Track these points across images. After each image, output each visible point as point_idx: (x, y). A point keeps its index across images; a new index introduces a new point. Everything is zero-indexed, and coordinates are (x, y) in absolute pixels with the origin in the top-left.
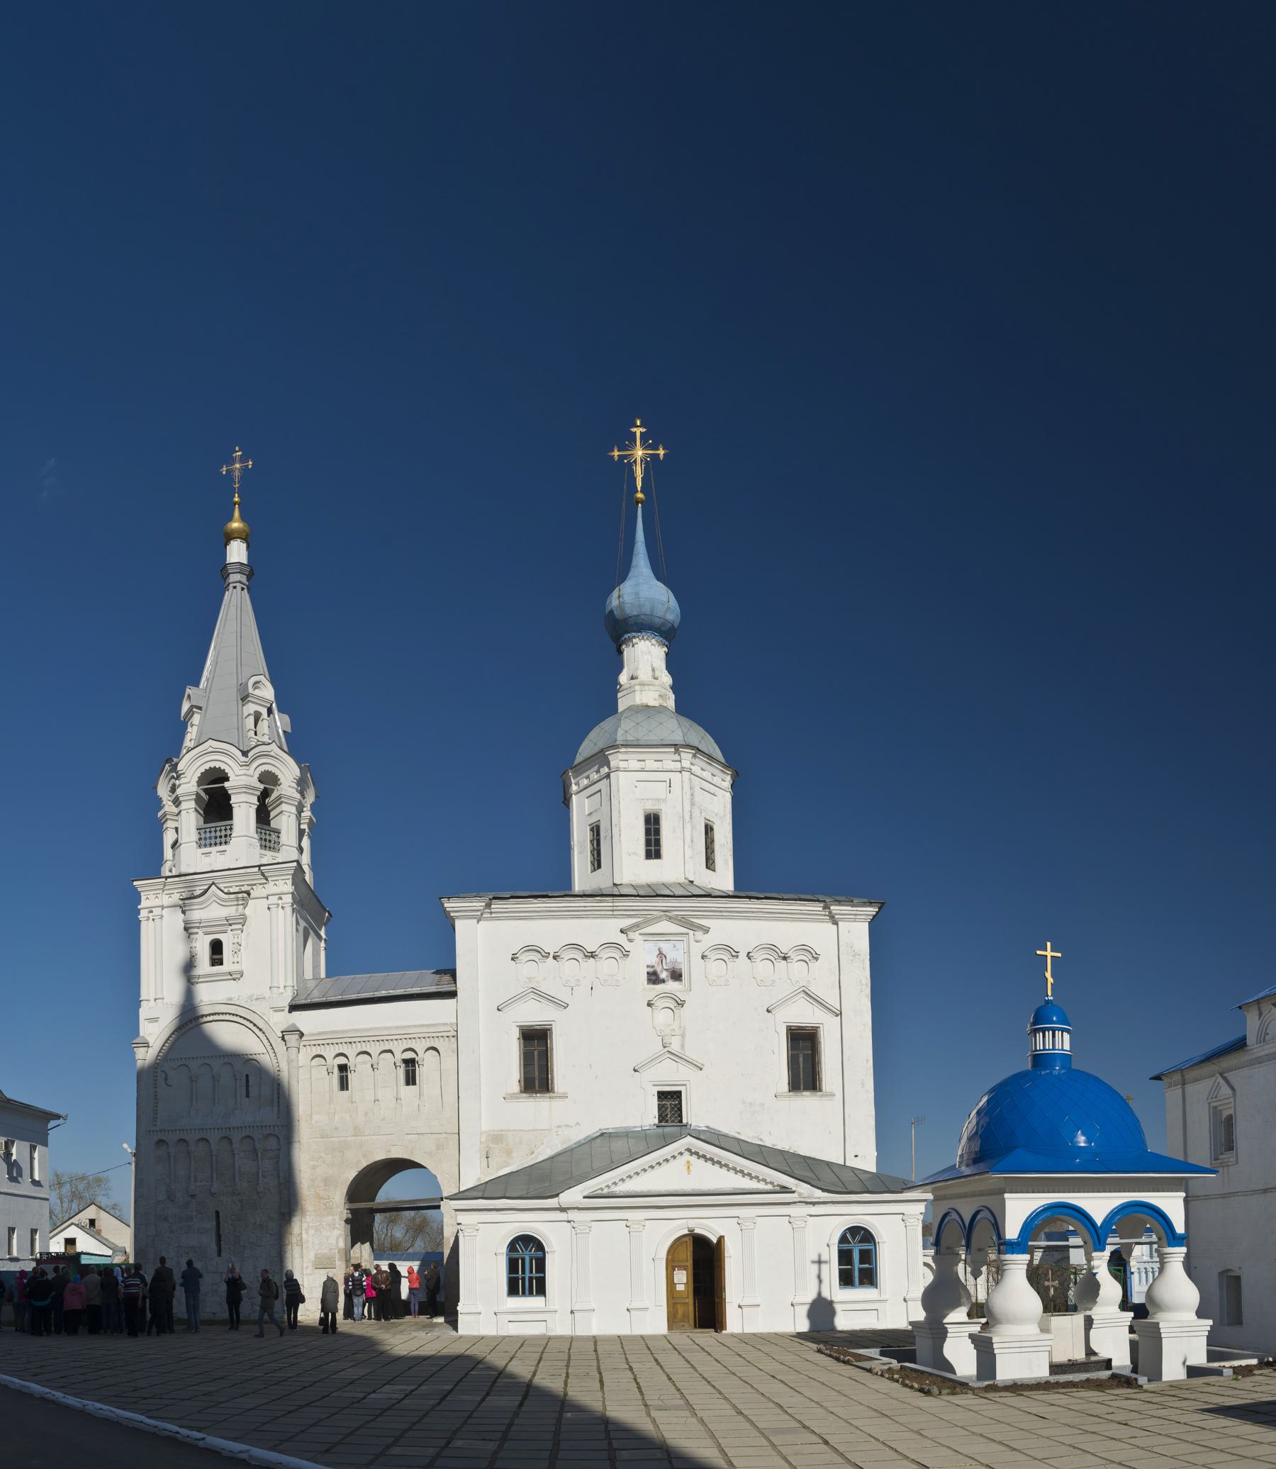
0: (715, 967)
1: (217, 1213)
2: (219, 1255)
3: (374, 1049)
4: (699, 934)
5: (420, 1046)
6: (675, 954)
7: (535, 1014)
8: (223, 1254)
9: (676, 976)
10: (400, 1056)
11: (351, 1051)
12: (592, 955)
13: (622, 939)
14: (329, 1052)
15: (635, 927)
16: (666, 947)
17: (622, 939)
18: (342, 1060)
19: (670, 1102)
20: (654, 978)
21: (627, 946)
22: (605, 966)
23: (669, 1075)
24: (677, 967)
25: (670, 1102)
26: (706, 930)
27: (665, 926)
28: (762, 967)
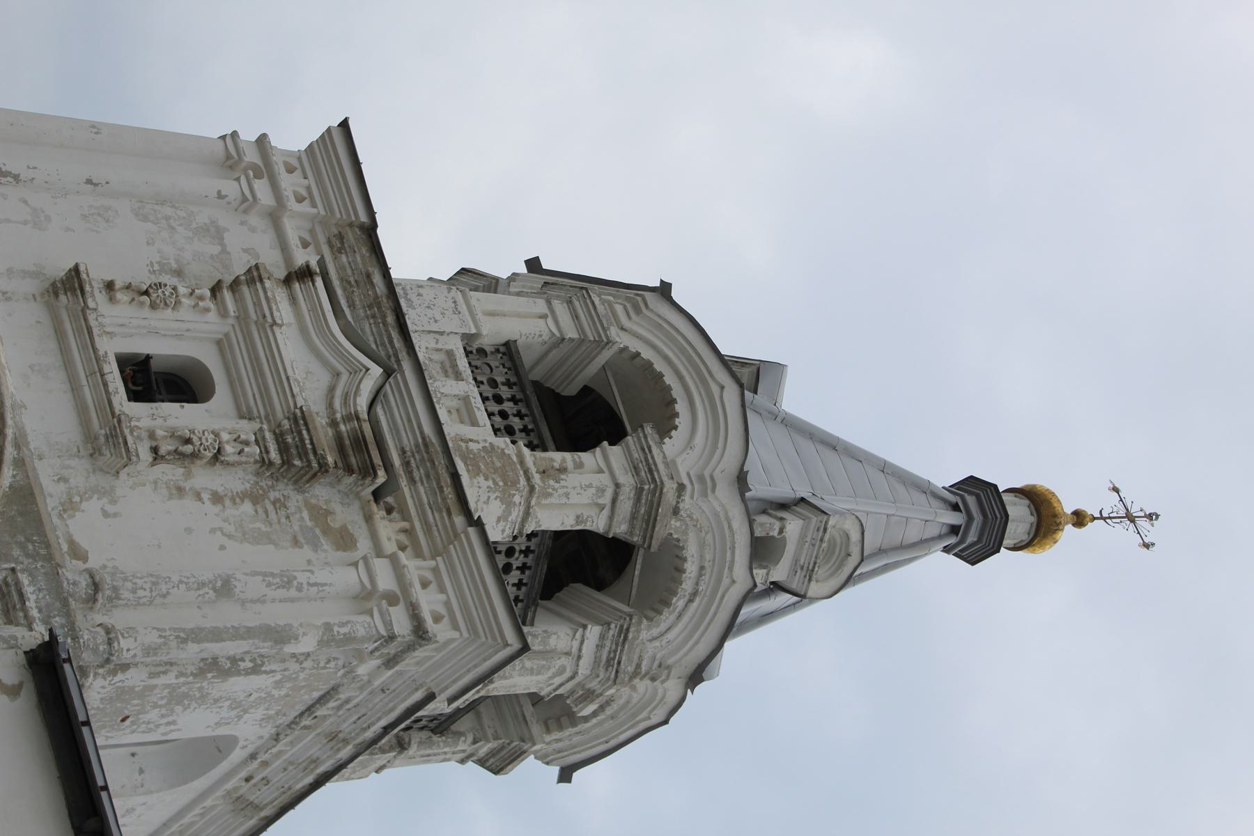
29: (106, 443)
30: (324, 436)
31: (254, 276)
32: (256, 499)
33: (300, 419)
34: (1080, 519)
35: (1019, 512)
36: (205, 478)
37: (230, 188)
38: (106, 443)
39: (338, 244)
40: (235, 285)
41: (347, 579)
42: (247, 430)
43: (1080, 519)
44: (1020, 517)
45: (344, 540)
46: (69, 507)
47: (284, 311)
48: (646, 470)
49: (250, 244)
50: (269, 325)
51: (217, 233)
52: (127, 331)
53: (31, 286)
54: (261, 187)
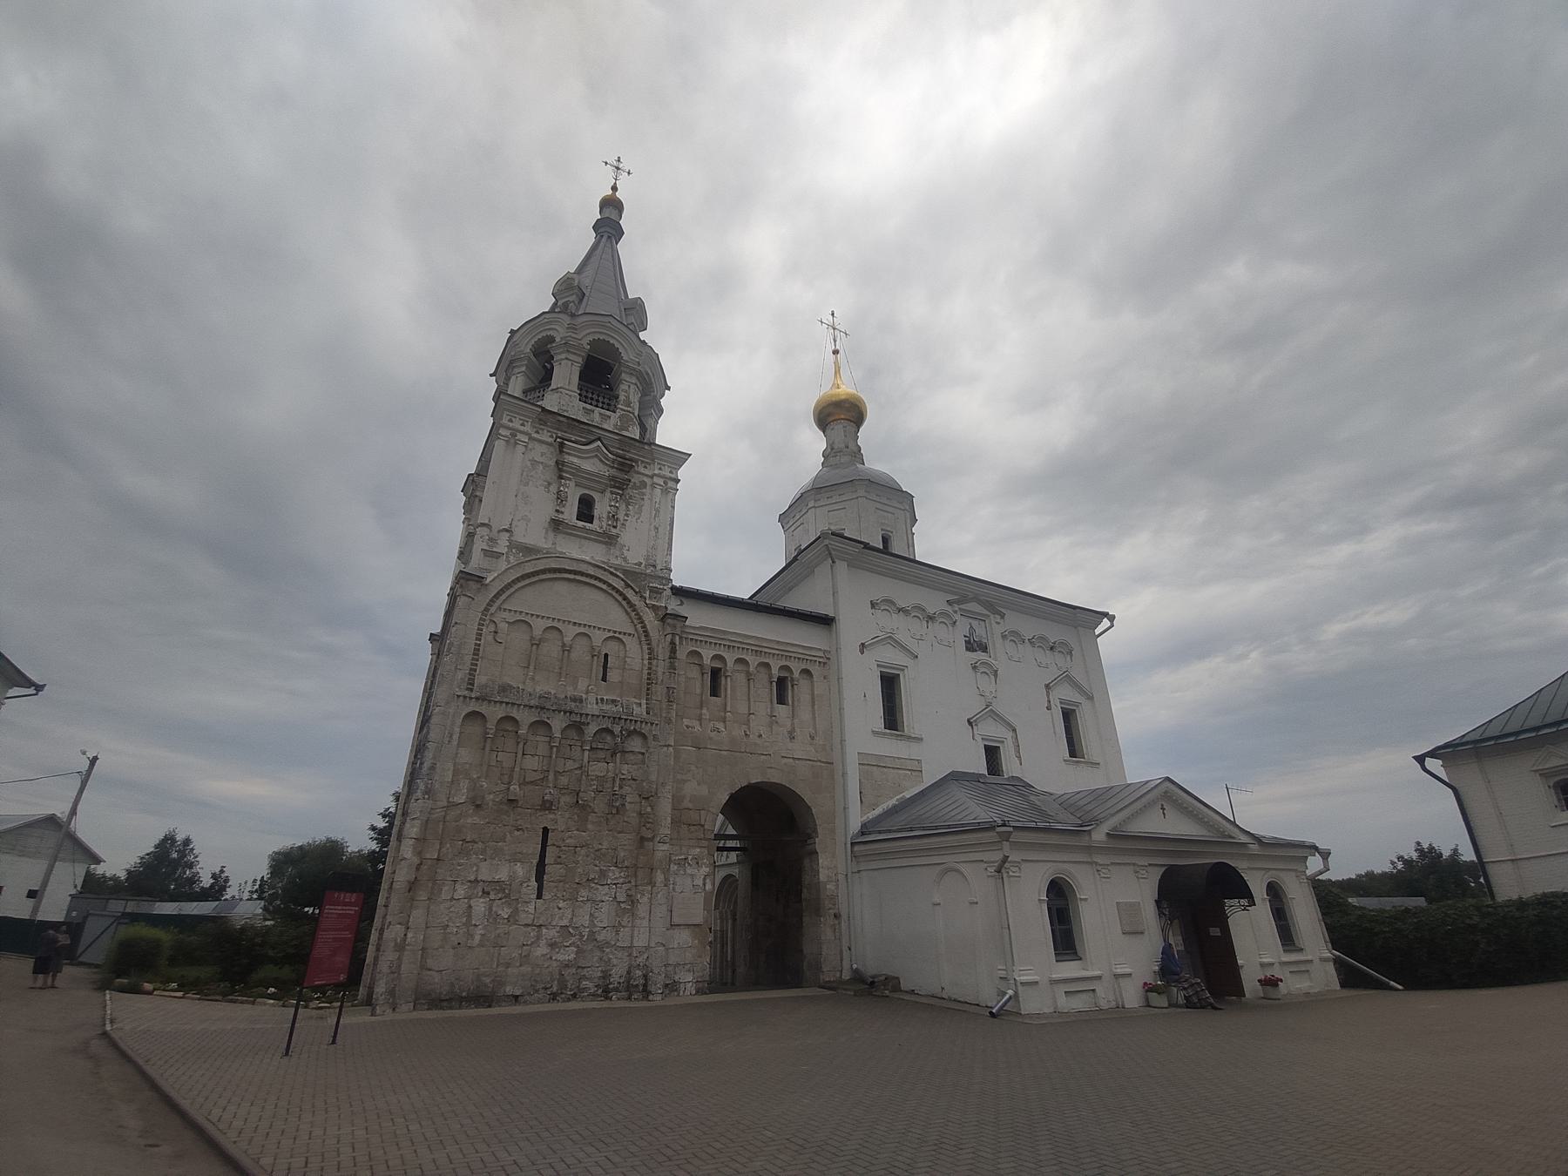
1: (546, 831)
2: (539, 896)
3: (753, 661)
5: (796, 668)
6: (980, 631)
7: (891, 656)
8: (546, 895)
9: (984, 649)
10: (775, 672)
11: (730, 658)
12: (931, 618)
13: (949, 609)
14: (707, 654)
15: (958, 602)
18: (718, 665)
22: (938, 629)
26: (1003, 616)
27: (974, 607)
28: (1046, 657)
29: (609, 540)
30: (613, 472)
31: (560, 466)
32: (628, 504)
33: (612, 478)
34: (614, 188)
35: (608, 213)
36: (621, 516)
37: (520, 449)
38: (609, 540)
39: (543, 422)
40: (560, 470)
41: (658, 491)
42: (608, 494)
43: (614, 188)
44: (608, 213)
45: (644, 485)
46: (625, 559)
47: (575, 460)
48: (633, 372)
49: (543, 454)
50: (579, 469)
51: (534, 463)
52: (570, 513)
53: (551, 535)
54: (519, 436)
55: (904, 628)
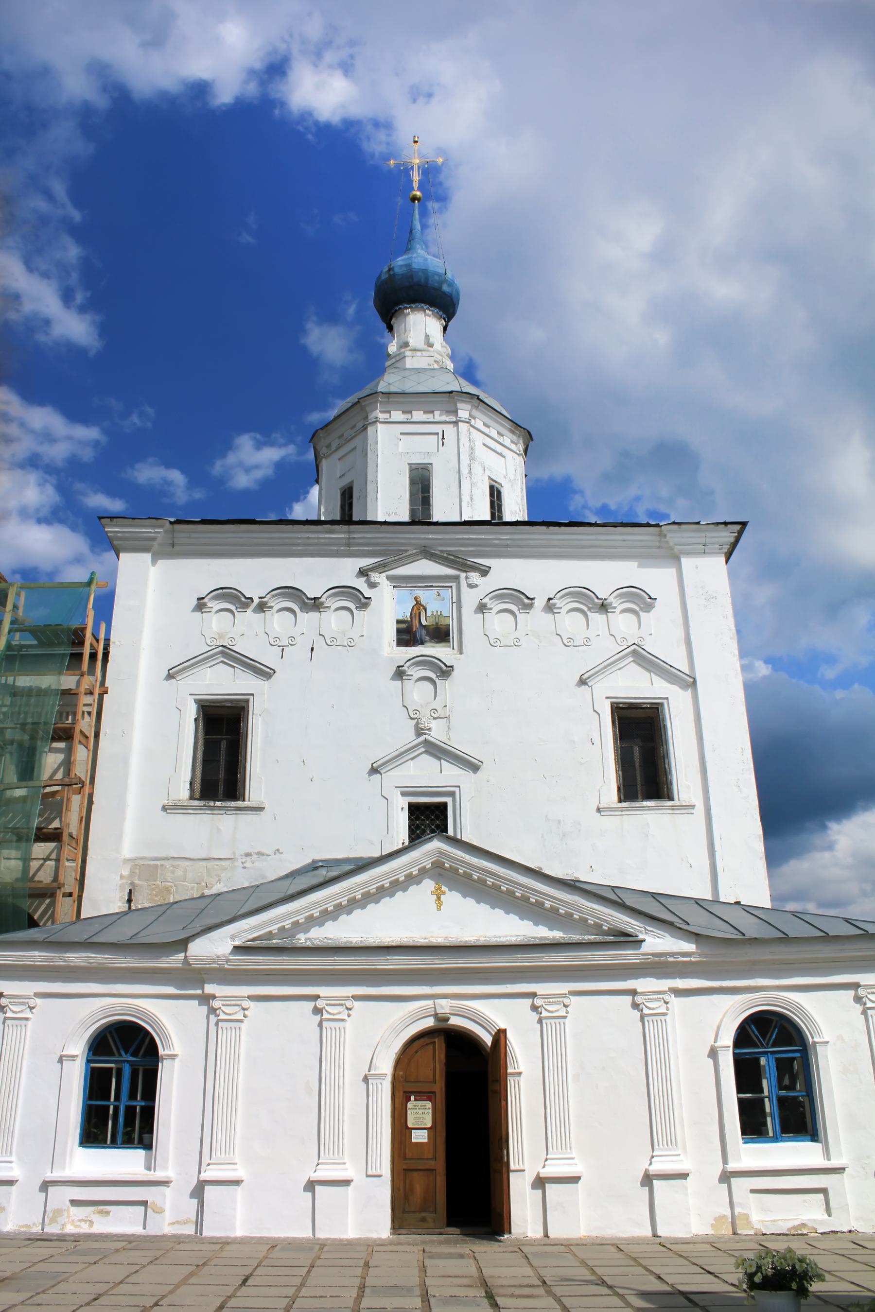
0: (498, 623)
4: (475, 577)
6: (437, 605)
7: (222, 683)
9: (441, 634)
12: (315, 605)
13: (360, 584)
15: (379, 568)
16: (426, 596)
17: (360, 584)
19: (428, 818)
20: (407, 635)
21: (367, 592)
22: (333, 620)
23: (427, 775)
24: (443, 622)
25: (428, 818)
26: (484, 572)
55: (248, 632)
